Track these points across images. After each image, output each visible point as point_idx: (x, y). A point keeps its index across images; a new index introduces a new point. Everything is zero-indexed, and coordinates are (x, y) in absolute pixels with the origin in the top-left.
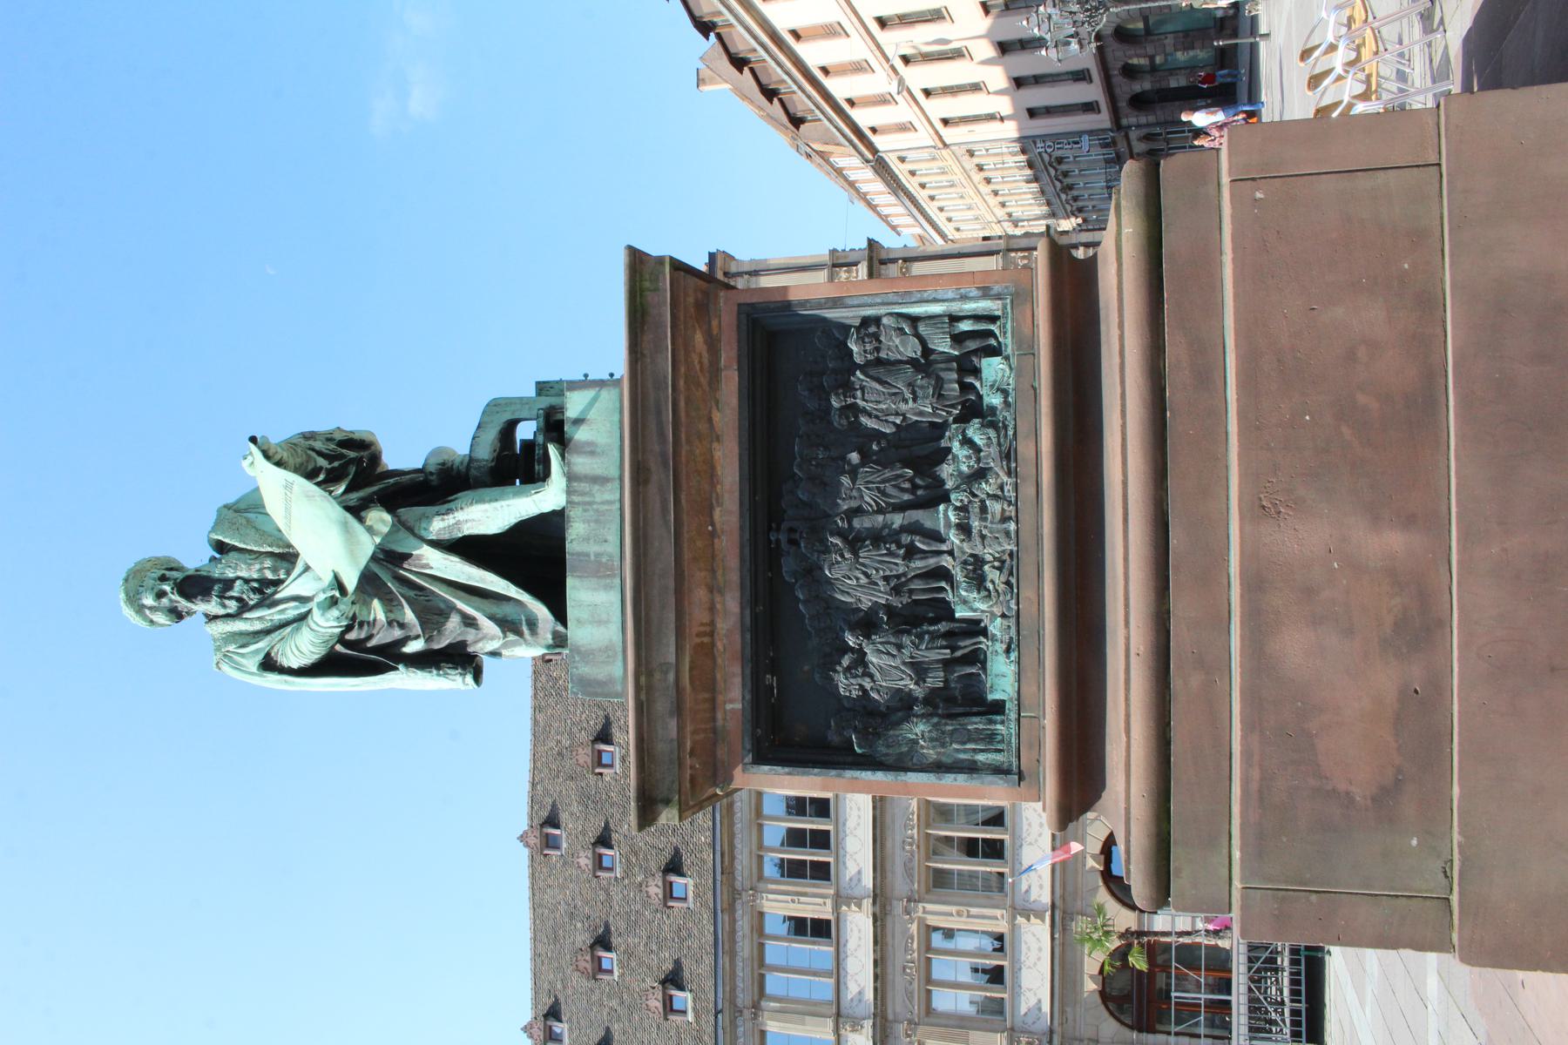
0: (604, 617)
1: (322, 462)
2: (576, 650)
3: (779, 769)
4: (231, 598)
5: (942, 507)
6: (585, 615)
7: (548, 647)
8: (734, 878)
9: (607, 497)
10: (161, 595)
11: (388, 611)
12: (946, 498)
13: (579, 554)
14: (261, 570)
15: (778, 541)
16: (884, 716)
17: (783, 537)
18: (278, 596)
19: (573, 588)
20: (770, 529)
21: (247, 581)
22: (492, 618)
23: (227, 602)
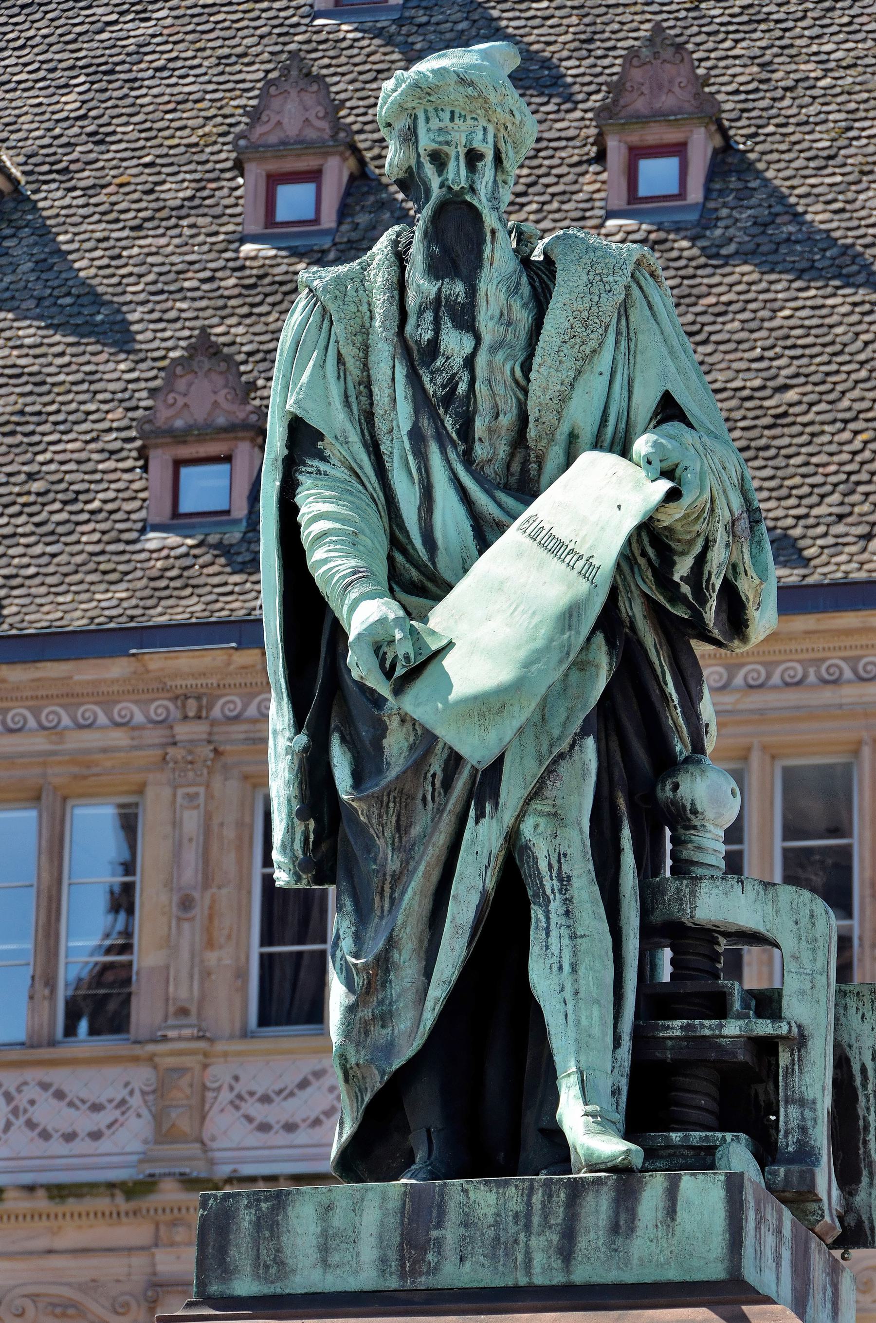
0: (334, 1258)
1: (683, 567)
6: (337, 1221)
9: (539, 1258)
21: (469, 362)
23: (429, 316)
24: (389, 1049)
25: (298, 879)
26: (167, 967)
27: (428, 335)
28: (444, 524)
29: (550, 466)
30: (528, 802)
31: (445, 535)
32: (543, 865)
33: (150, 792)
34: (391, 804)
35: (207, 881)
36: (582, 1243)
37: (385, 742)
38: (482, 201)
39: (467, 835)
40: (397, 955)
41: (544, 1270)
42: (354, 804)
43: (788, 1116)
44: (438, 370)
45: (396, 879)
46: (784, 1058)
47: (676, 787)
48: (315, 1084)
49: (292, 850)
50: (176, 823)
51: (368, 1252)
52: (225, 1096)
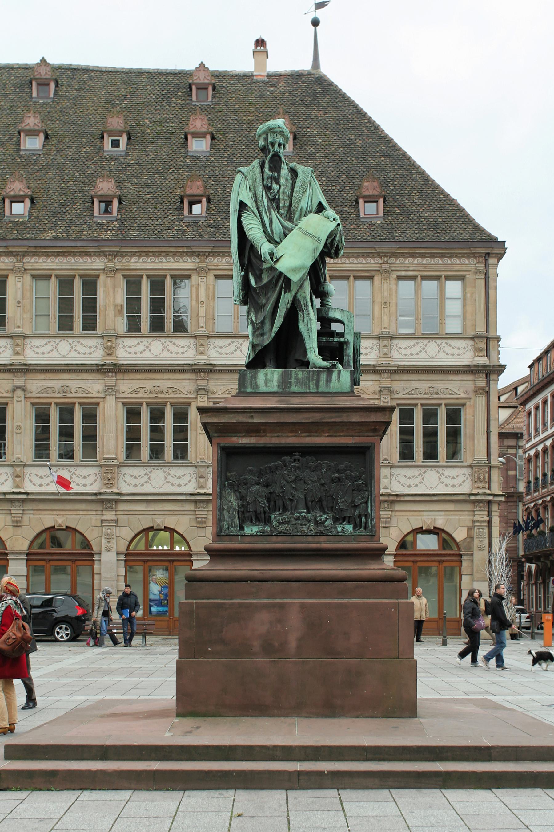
0: (268, 385)
2: (256, 374)
3: (219, 456)
5: (305, 511)
6: (269, 377)
8: (32, 256)
9: (311, 386)
10: (273, 144)
11: (267, 269)
12: (308, 512)
13: (291, 375)
14: (284, 199)
15: (295, 455)
16: (238, 491)
17: (297, 457)
18: (272, 210)
19: (278, 372)
20: (299, 452)
21: (279, 191)
22: (264, 318)
23: (270, 180)
24: (263, 341)
26: (15, 317)
27: (269, 185)
28: (275, 227)
29: (296, 216)
30: (298, 290)
31: (275, 230)
32: (302, 303)
33: (9, 277)
35: (23, 298)
36: (320, 384)
38: (281, 154)
39: (282, 296)
41: (313, 389)
43: (345, 358)
44: (272, 193)
45: (265, 305)
46: (345, 347)
47: (324, 288)
48: (49, 344)
50: (16, 285)
51: (275, 383)
52: (29, 346)
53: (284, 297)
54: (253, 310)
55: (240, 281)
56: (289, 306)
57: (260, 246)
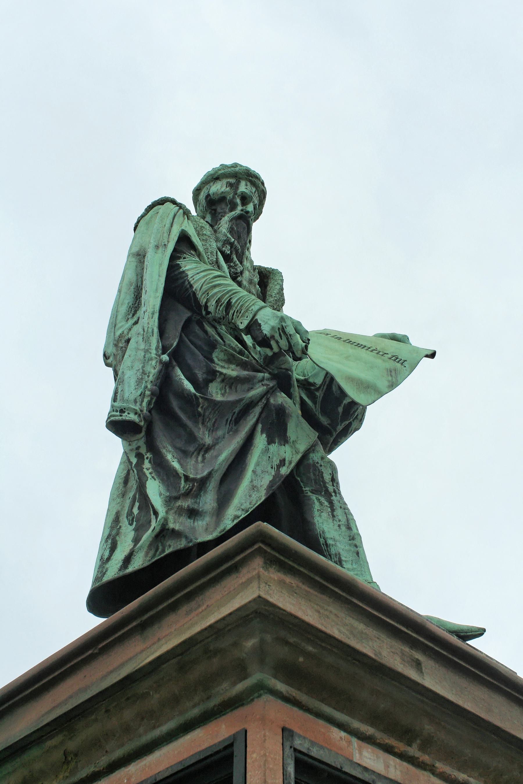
4: (231, 252)
7: (166, 520)
22: (210, 474)
25: (141, 421)
34: (217, 412)
37: (210, 385)
40: (208, 484)
42: (201, 400)
44: (231, 266)
49: (141, 405)
53: (267, 450)
54: (170, 448)
55: (153, 371)
56: (285, 471)
57: (255, 308)
